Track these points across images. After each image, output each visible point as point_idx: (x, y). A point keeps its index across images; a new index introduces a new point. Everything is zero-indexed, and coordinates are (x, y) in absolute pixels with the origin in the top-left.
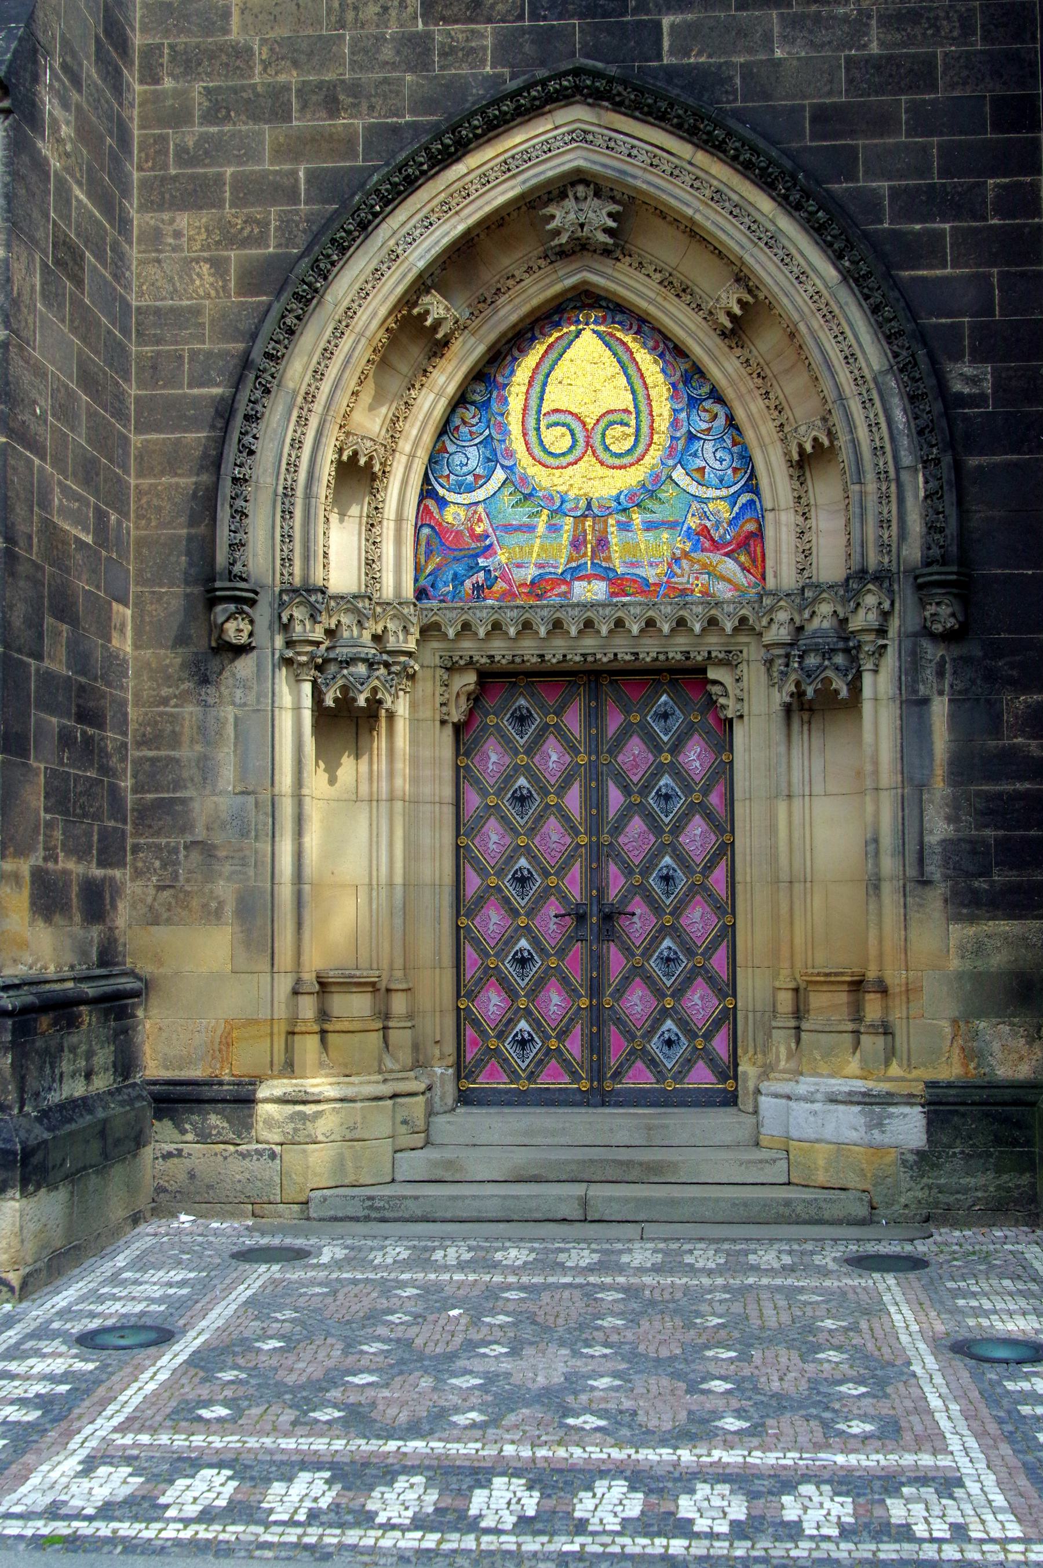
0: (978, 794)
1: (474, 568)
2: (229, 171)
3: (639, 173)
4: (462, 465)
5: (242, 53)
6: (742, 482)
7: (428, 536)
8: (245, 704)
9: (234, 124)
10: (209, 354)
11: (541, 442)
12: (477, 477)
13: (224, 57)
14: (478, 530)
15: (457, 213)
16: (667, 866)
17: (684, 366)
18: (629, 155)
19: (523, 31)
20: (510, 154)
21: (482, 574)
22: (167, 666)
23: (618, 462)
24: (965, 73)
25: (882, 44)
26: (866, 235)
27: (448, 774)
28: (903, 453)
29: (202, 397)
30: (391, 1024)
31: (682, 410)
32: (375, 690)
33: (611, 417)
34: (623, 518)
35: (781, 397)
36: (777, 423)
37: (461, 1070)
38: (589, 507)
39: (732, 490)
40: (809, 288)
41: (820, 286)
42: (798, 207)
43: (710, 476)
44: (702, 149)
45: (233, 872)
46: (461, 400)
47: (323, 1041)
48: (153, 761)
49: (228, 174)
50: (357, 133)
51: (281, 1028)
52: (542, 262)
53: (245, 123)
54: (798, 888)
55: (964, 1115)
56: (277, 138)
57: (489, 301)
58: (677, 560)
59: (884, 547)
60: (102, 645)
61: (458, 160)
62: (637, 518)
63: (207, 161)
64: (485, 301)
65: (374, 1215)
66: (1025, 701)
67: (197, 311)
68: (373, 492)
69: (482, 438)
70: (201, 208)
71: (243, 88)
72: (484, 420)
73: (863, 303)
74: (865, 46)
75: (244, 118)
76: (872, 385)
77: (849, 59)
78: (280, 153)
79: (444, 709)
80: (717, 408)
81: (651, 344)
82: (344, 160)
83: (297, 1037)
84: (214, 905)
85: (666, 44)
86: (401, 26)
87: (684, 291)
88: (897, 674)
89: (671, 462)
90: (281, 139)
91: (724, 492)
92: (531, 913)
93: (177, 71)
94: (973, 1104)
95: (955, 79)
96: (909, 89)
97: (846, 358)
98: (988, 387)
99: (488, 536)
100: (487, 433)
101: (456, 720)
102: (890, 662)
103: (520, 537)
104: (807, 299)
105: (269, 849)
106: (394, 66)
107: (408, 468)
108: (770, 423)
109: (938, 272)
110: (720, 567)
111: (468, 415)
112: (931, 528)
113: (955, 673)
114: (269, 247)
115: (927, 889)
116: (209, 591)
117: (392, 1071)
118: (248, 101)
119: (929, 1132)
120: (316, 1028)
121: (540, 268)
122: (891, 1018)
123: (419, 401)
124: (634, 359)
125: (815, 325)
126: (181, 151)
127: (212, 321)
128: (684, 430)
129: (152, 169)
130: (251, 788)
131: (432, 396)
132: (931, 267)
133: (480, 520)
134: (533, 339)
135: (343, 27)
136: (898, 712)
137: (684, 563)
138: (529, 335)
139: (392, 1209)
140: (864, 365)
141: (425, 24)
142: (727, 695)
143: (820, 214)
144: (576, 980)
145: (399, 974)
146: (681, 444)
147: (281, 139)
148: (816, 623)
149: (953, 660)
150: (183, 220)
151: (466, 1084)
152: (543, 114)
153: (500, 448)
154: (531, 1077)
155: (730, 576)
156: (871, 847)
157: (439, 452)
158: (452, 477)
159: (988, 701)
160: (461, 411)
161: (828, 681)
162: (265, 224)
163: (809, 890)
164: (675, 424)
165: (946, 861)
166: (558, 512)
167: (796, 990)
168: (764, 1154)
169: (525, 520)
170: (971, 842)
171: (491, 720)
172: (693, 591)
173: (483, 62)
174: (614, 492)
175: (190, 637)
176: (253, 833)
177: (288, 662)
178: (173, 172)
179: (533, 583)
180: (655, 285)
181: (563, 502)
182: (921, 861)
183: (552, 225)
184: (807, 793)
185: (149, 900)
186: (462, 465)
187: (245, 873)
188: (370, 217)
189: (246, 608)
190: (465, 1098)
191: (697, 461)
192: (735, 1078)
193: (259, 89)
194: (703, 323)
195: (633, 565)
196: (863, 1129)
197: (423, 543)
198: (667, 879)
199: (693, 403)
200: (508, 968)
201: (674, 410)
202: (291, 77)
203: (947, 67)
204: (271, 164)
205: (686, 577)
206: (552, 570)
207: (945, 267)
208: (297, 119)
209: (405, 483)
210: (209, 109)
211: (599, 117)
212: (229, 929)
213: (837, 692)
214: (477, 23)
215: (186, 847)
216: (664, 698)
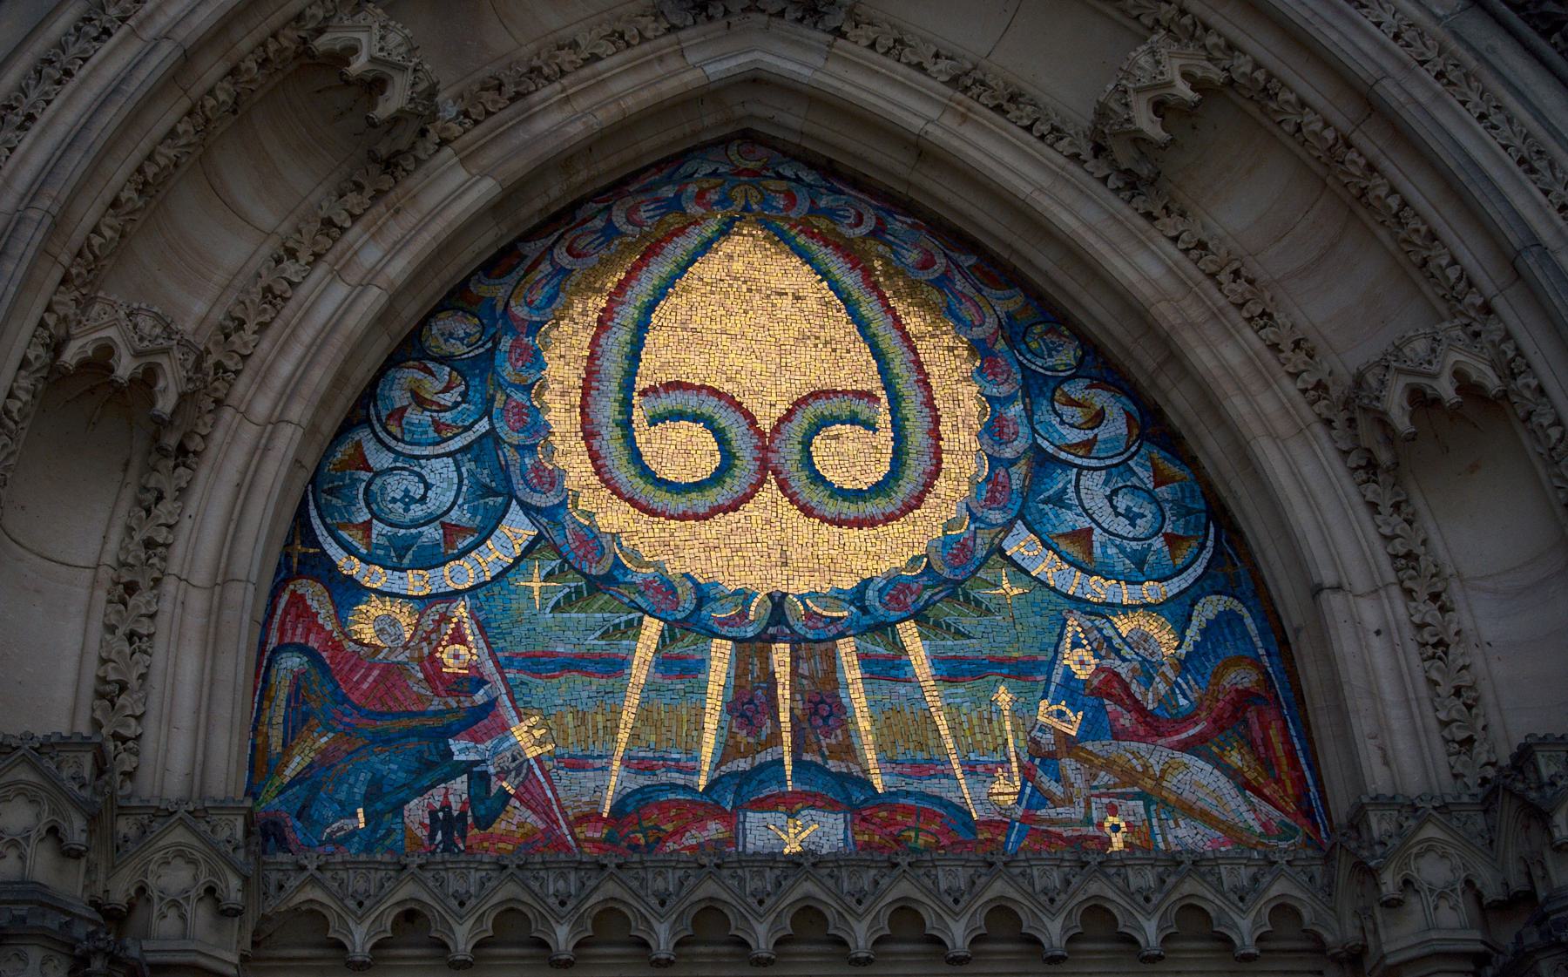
1: (440, 766)
7: (298, 679)
12: (451, 531)
14: (451, 666)
17: (1007, 303)
21: (460, 784)
33: (823, 407)
52: (650, 26)
64: (499, 88)
68: (149, 501)
69: (469, 437)
87: (1013, 98)
91: (1151, 591)
99: (481, 682)
100: (483, 426)
103: (581, 687)
104: (1388, 40)
107: (261, 450)
108: (1286, 382)
110: (1170, 783)
111: (431, 387)
121: (643, 39)
123: (303, 290)
125: (1422, 96)
128: (1020, 444)
131: (340, 292)
133: (459, 638)
137: (1068, 765)
138: (598, 223)
155: (1206, 802)
158: (378, 527)
160: (409, 375)
164: (994, 430)
169: (593, 642)
174: (848, 583)
180: (938, 88)
186: (408, 500)
191: (1068, 515)
194: (1072, 167)
199: (1036, 387)
201: (990, 399)
206: (679, 779)
209: (245, 489)
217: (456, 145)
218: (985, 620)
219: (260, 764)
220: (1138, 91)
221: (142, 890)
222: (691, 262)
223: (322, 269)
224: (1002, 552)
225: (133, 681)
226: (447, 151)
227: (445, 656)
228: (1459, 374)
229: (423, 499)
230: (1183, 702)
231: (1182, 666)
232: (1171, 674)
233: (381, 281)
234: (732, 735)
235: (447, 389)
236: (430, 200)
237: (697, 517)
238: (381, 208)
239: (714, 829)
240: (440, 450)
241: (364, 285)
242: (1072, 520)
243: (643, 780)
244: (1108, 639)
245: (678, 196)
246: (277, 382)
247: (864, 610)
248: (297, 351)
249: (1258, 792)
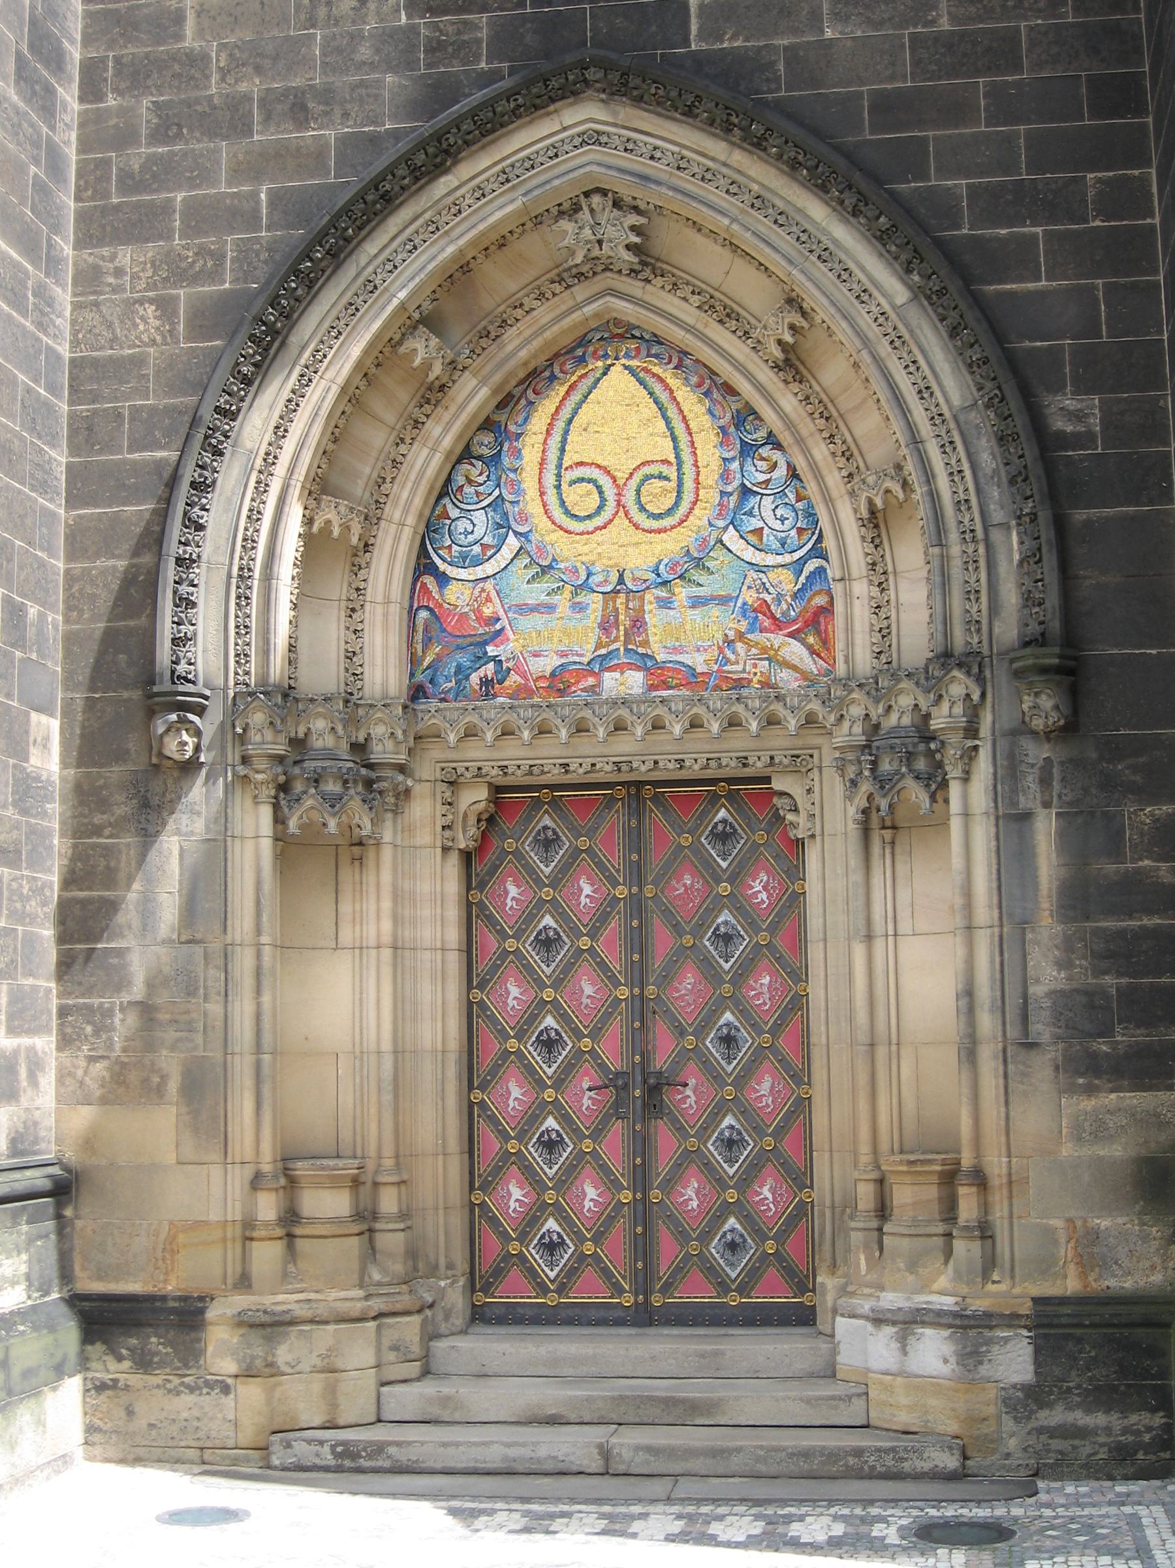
0: (1096, 932)
1: (481, 659)
2: (180, 197)
3: (664, 177)
4: (467, 533)
5: (197, 61)
6: (809, 545)
7: (426, 620)
8: (192, 833)
9: (187, 143)
10: (153, 410)
11: (562, 503)
12: (485, 547)
13: (176, 67)
14: (487, 611)
15: (446, 232)
16: (727, 1025)
18: (652, 158)
19: (524, 18)
20: (509, 161)
22: (102, 787)
23: (655, 524)
24: (1055, 50)
25: (953, 19)
26: (939, 244)
27: (453, 913)
28: (992, 507)
29: (145, 462)
30: (378, 1226)
31: (733, 459)
33: (647, 470)
34: (663, 593)
35: (849, 439)
36: (844, 473)
38: (621, 581)
39: (797, 555)
40: (873, 308)
41: (886, 307)
42: (855, 213)
43: (769, 539)
44: (740, 147)
45: (178, 1040)
46: (466, 455)
47: (291, 1248)
48: (83, 903)
49: (179, 199)
50: (327, 144)
53: (199, 141)
54: (881, 1052)
55: (1079, 1340)
56: (235, 156)
57: (493, 335)
58: (730, 643)
59: (973, 624)
60: (15, 766)
61: (447, 171)
62: (683, 592)
63: (155, 186)
65: (347, 1463)
66: (1152, 814)
67: (138, 362)
69: (491, 499)
70: (147, 240)
71: (197, 101)
72: (493, 477)
73: (939, 325)
74: (933, 22)
75: (198, 135)
76: (952, 425)
77: (914, 38)
78: (238, 173)
79: (448, 833)
80: (776, 455)
81: (694, 380)
82: (312, 177)
83: (255, 1244)
84: (157, 1080)
85: (694, 28)
86: (382, 20)
87: (728, 315)
88: (991, 782)
89: (721, 524)
90: (241, 157)
91: (788, 558)
92: (559, 1083)
93: (123, 85)
94: (1093, 1325)
95: (1044, 57)
96: (989, 70)
97: (920, 392)
98: (1095, 423)
99: (499, 619)
101: (462, 846)
102: (983, 766)
103: (537, 620)
104: (871, 321)
105: (222, 1011)
106: (373, 67)
108: (836, 473)
109: (1031, 286)
111: (474, 472)
112: (1028, 600)
113: (1063, 780)
114: (224, 282)
115: (1033, 1053)
117: (380, 1284)
118: (204, 114)
119: (1037, 1363)
120: (279, 1232)
121: (554, 295)
122: (990, 1218)
123: (409, 457)
124: (675, 399)
126: (126, 177)
127: (158, 373)
128: (736, 483)
129: (92, 199)
130: (198, 936)
131: (425, 451)
132: (1021, 279)
133: (488, 599)
134: (553, 378)
135: (313, 26)
136: (993, 830)
137: (739, 646)
138: (547, 374)
139: (370, 1457)
140: (941, 400)
141: (409, 17)
142: (796, 810)
143: (882, 219)
144: (617, 1169)
145: (388, 1163)
146: (733, 500)
147: (241, 157)
148: (893, 719)
149: (1062, 763)
150: (126, 256)
151: (480, 1298)
152: (549, 114)
153: (512, 510)
154: (561, 1290)
155: (796, 662)
156: (963, 1002)
157: (439, 517)
158: (455, 547)
159: (1105, 814)
162: (219, 257)
163: (894, 1055)
164: (725, 476)
165: (1057, 1016)
166: (584, 587)
168: (838, 1389)
169: (543, 598)
170: (1086, 993)
171: (510, 844)
172: (750, 681)
173: (477, 59)
175: (127, 752)
176: (202, 991)
178: (115, 201)
179: (553, 674)
181: (589, 575)
182: (1025, 1018)
184: (891, 932)
185: (80, 1073)
186: (467, 533)
187: (192, 1041)
188: (341, 242)
189: (191, 717)
193: (216, 101)
195: (676, 650)
196: (953, 1360)
197: (420, 629)
198: (728, 1041)
199: (747, 450)
200: (533, 1153)
201: (724, 460)
202: (252, 86)
203: (1032, 44)
204: (229, 184)
205: (742, 662)
206: (577, 659)
207: (1039, 279)
208: (259, 133)
209: (393, 556)
210: (158, 126)
211: (615, 114)
212: (174, 1110)
214: (470, 12)
215: (122, 1010)
216: (722, 813)
217: (471, 368)
218: (711, 577)
219: (414, 661)
222: (590, 392)
223: (416, 444)
224: (721, 542)
225: (358, 651)
226: (467, 373)
227: (485, 609)
229: (472, 532)
230: (793, 613)
231: (795, 596)
232: (789, 600)
233: (441, 449)
234: (600, 638)
235: (480, 475)
236: (460, 399)
237: (588, 533)
238: (439, 409)
239: (591, 681)
240: (478, 506)
241: (434, 450)
242: (756, 523)
243: (564, 660)
244: (764, 584)
245: (584, 354)
246: (402, 502)
247: (658, 575)
248: (409, 485)
249: (818, 655)
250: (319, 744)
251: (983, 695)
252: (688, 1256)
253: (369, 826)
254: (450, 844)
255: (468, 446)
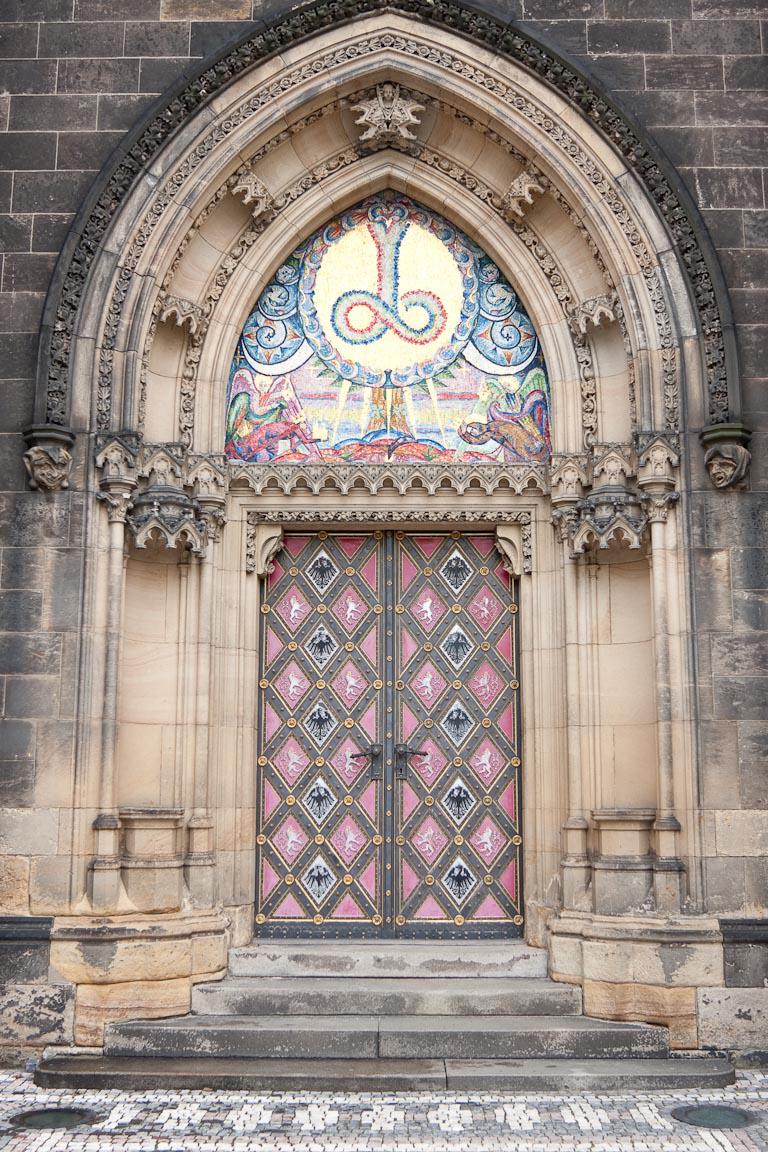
30: (191, 863)
32: (184, 534)
37: (264, 905)
46: (273, 281)
51: (80, 864)
79: (251, 561)
92: (330, 752)
101: (261, 572)
116: (25, 434)
148: (605, 479)
154: (326, 911)
161: (618, 532)
167: (586, 830)
177: (103, 502)
183: (361, 120)
190: (260, 932)
192: (523, 913)
213: (628, 543)
216: (456, 554)
220: (513, 197)
221: (196, 479)
228: (602, 314)
250: (160, 481)
251: (679, 460)
252: (424, 887)
253: (199, 543)
254: (252, 569)
255: (275, 276)
